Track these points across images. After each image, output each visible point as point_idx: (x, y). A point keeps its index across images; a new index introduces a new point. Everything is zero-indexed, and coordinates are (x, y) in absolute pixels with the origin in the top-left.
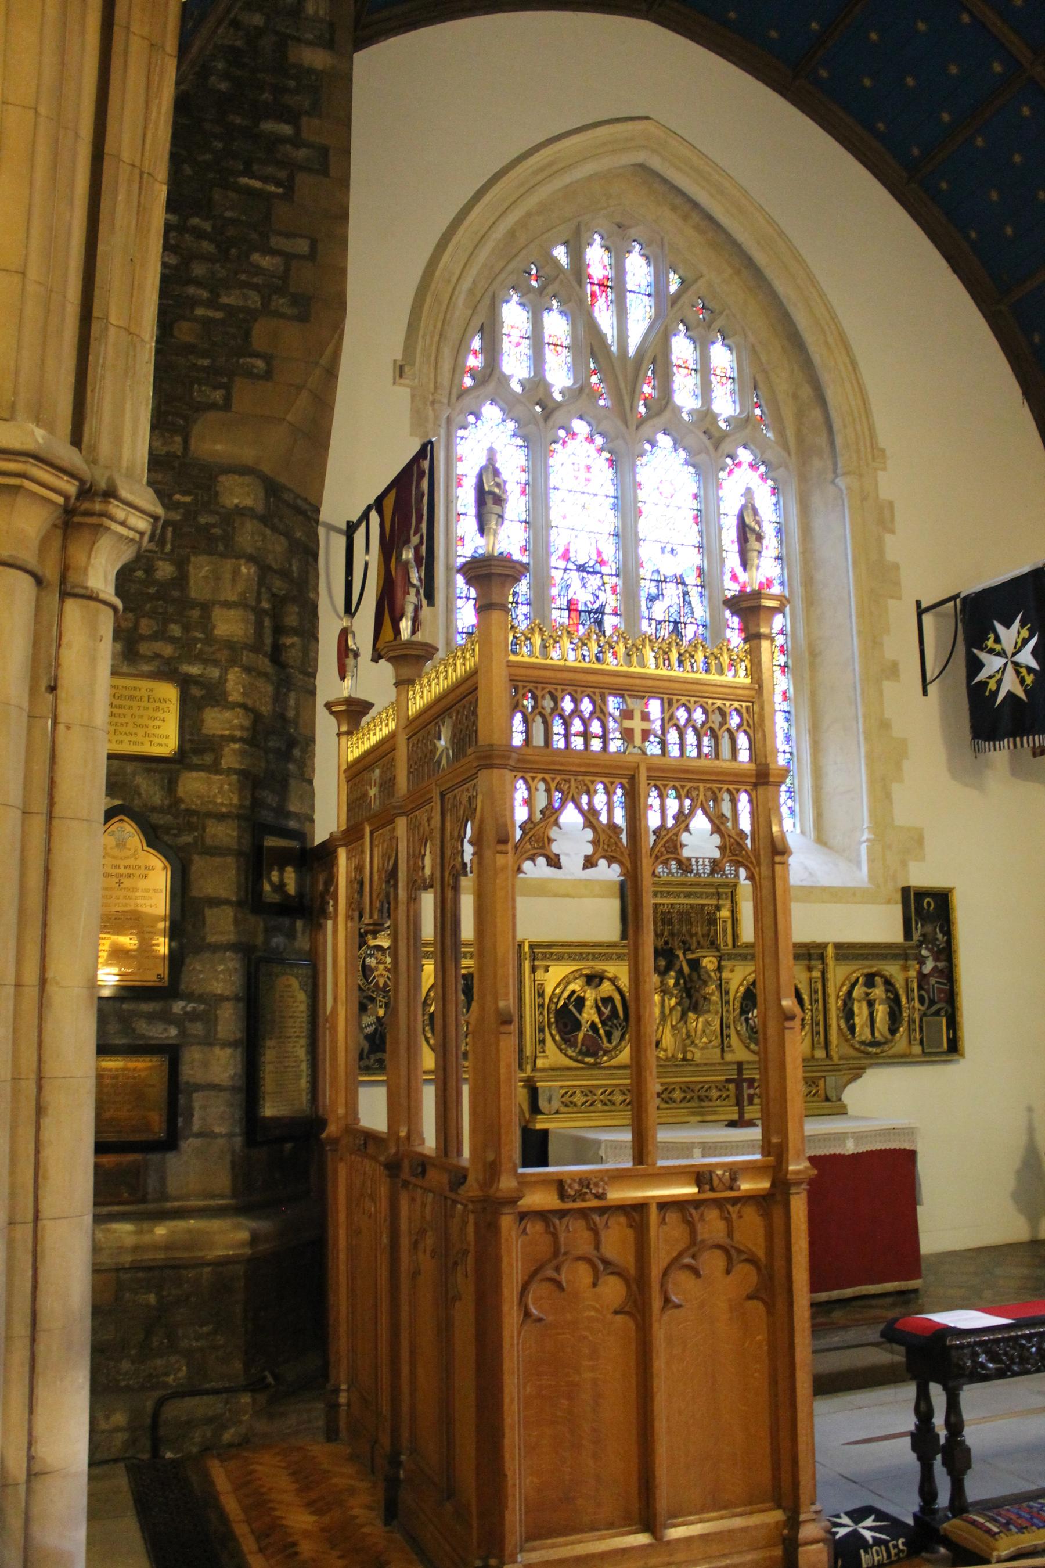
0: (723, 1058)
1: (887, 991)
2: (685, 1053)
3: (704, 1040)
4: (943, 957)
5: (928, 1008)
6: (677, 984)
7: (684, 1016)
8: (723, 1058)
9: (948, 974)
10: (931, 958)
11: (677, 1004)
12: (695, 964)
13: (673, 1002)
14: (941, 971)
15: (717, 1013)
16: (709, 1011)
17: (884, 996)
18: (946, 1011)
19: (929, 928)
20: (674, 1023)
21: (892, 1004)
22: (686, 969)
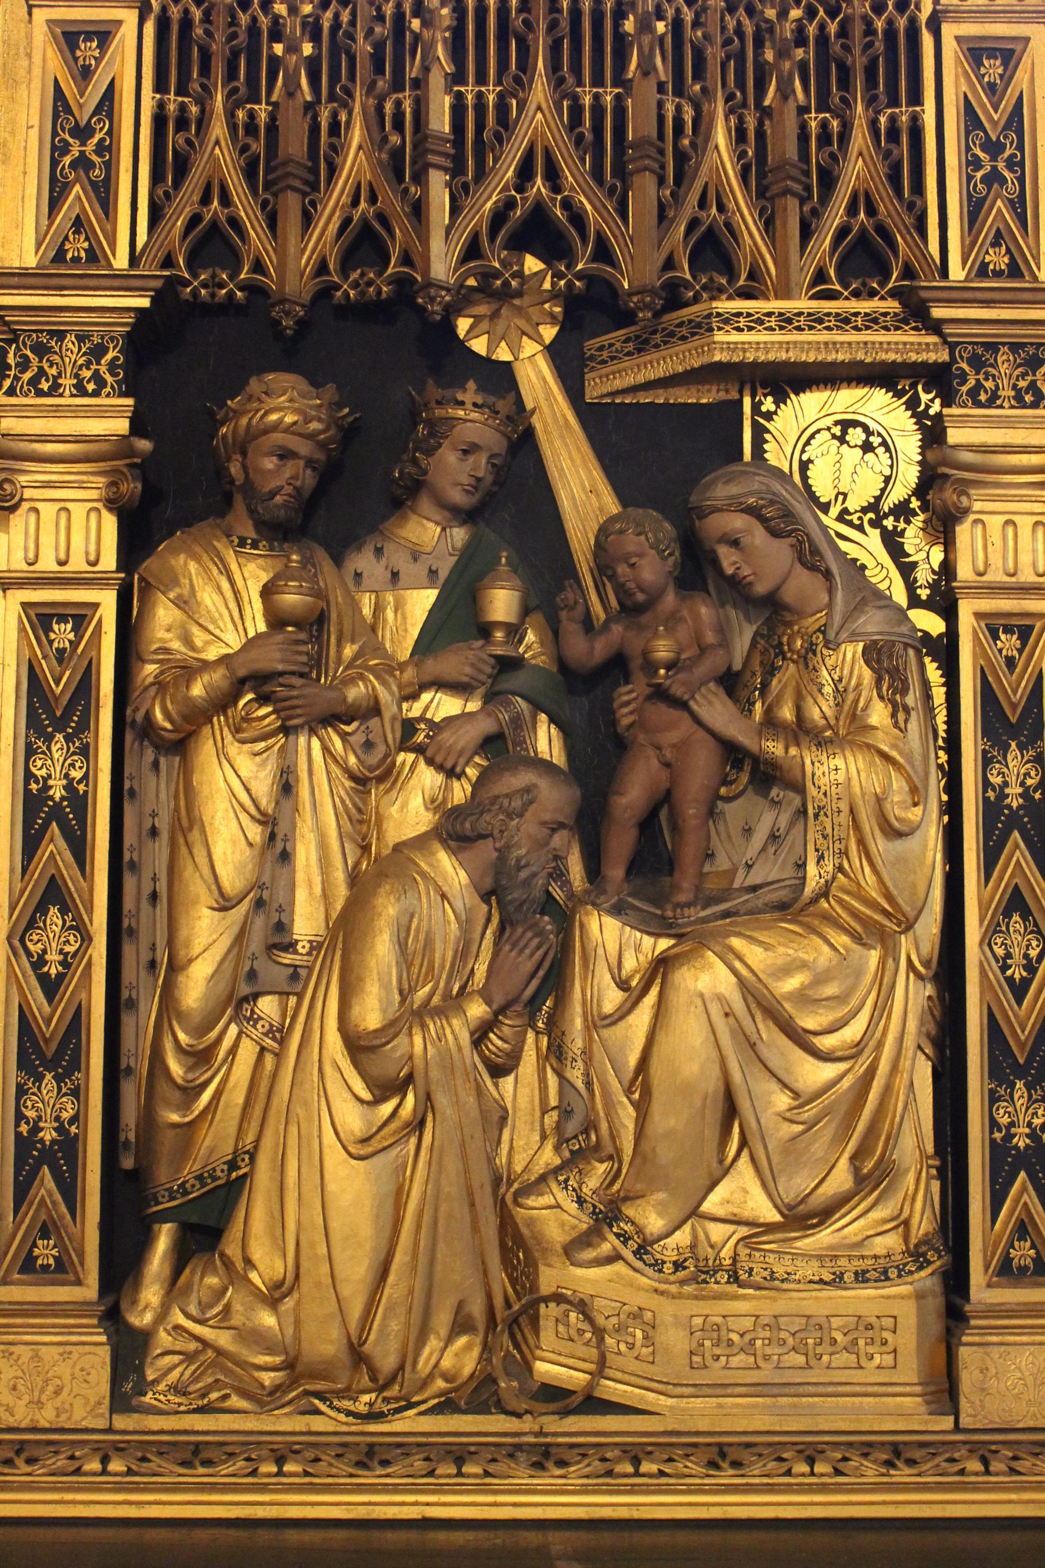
0: (945, 1388)
2: (513, 1319)
3: (741, 1193)
6: (458, 617)
7: (534, 926)
8: (945, 1388)
11: (455, 829)
12: (681, 450)
13: (412, 805)
15: (882, 926)
16: (791, 907)
20: (371, 1016)
22: (581, 488)
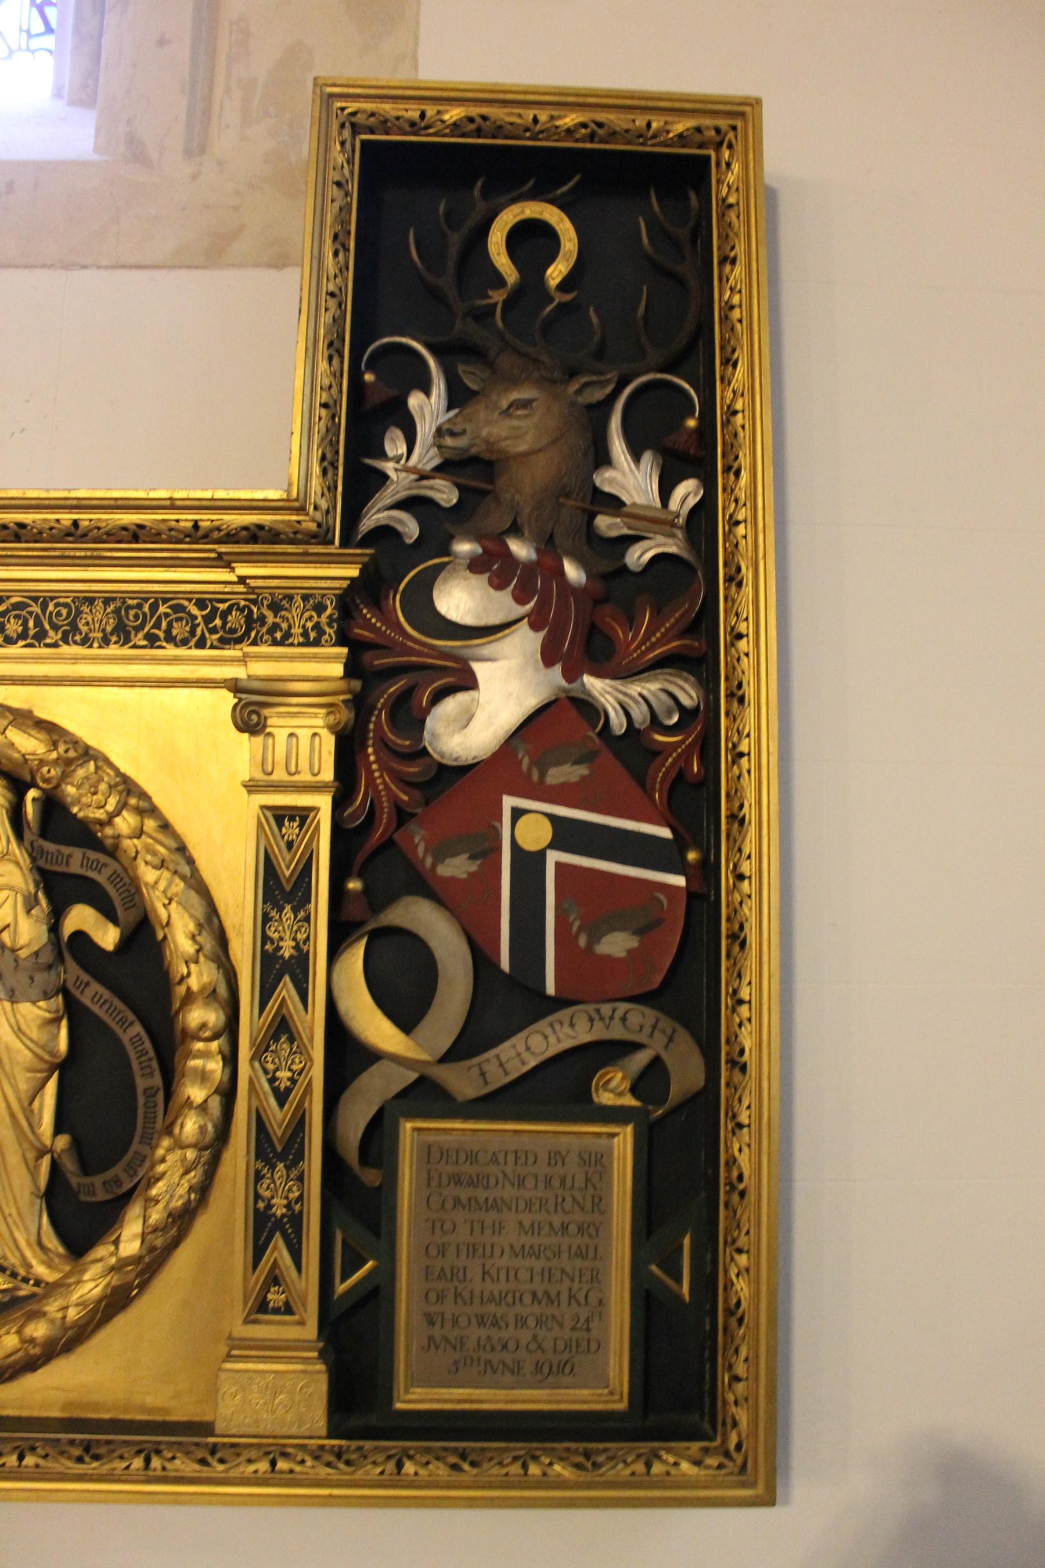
1: (57, 890)
4: (643, 633)
5: (462, 1049)
9: (685, 788)
10: (524, 642)
14: (633, 748)
17: (29, 932)
18: (651, 1081)
19: (520, 424)
21: (94, 995)
